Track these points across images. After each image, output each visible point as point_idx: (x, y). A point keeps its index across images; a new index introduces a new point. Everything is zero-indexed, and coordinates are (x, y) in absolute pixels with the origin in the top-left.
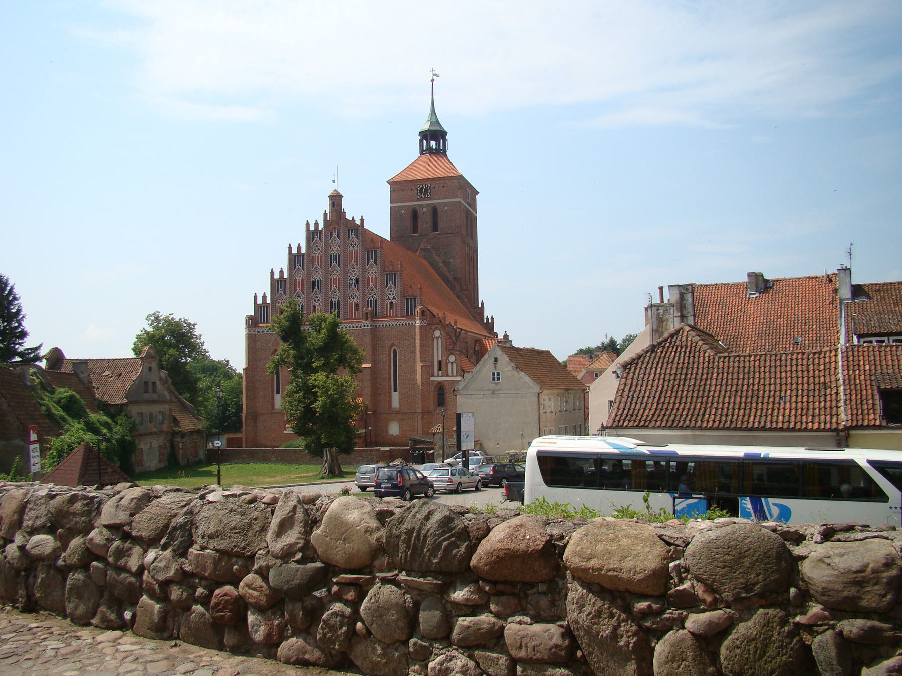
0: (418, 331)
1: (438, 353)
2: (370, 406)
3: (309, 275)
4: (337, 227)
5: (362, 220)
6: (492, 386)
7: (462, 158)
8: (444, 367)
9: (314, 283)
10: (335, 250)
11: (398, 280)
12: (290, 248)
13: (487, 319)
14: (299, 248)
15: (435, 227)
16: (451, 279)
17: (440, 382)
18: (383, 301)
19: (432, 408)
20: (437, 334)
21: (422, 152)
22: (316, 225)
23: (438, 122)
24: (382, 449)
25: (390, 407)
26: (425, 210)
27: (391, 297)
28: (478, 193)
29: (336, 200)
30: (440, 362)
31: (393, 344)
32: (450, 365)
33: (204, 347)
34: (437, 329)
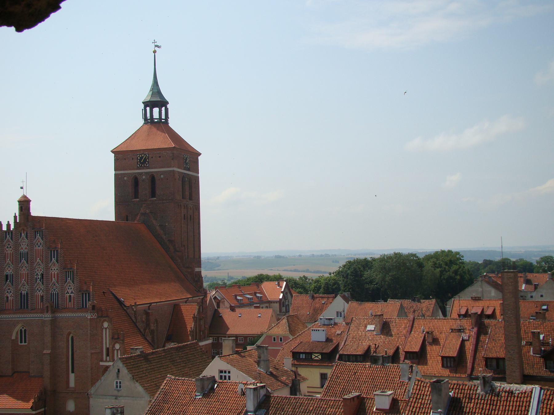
1: (106, 342)
4: (25, 228)
7: (183, 122)
8: (110, 354)
9: (7, 276)
10: (24, 248)
15: (153, 194)
23: (159, 93)
26: (144, 177)
27: (70, 291)
28: (200, 154)
29: (24, 204)
30: (108, 349)
32: (116, 352)
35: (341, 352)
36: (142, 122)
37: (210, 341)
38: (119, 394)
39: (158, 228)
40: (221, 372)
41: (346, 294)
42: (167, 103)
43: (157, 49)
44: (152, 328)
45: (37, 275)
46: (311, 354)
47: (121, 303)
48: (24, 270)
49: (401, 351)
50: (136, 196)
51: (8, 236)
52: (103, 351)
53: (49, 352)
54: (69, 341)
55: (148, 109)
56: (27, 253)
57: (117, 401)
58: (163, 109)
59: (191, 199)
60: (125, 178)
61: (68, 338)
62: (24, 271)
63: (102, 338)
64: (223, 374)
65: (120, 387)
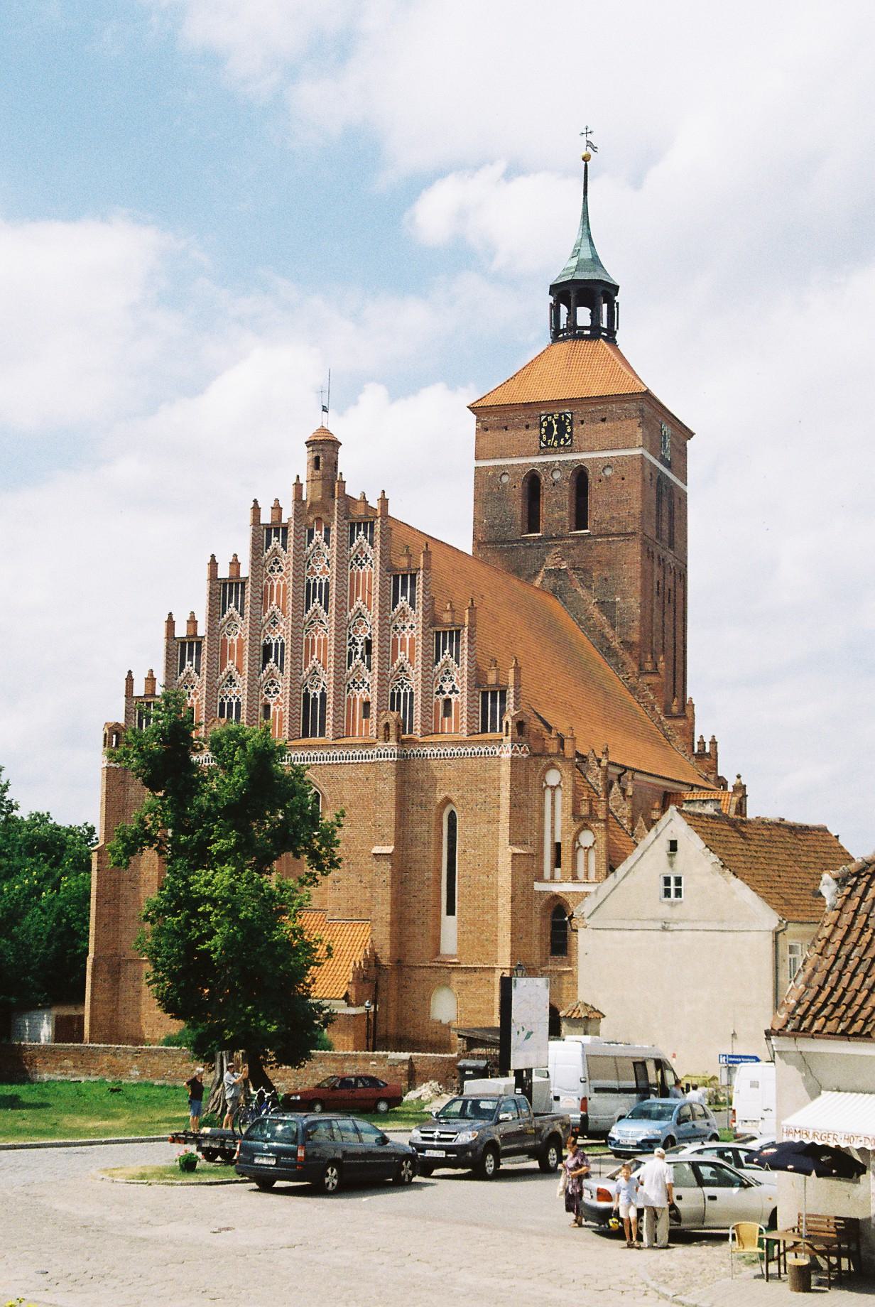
0: (505, 770)
4: (324, 516)
5: (384, 501)
6: (663, 909)
7: (650, 348)
9: (267, 650)
11: (465, 645)
12: (213, 564)
13: (702, 743)
14: (235, 564)
15: (581, 519)
16: (615, 644)
17: (556, 897)
18: (426, 695)
19: (536, 959)
20: (553, 778)
21: (557, 334)
23: (595, 260)
24: (393, 1055)
25: (438, 953)
26: (557, 476)
27: (447, 687)
28: (692, 434)
29: (324, 450)
30: (558, 847)
31: (448, 801)
32: (581, 854)
33: (8, 796)
34: (552, 766)
38: (676, 913)
42: (616, 288)
45: (354, 643)
48: (316, 630)
50: (533, 527)
51: (274, 539)
52: (542, 852)
54: (441, 824)
56: (327, 584)
57: (668, 934)
59: (671, 545)
60: (505, 479)
61: (441, 814)
63: (542, 815)
65: (678, 893)
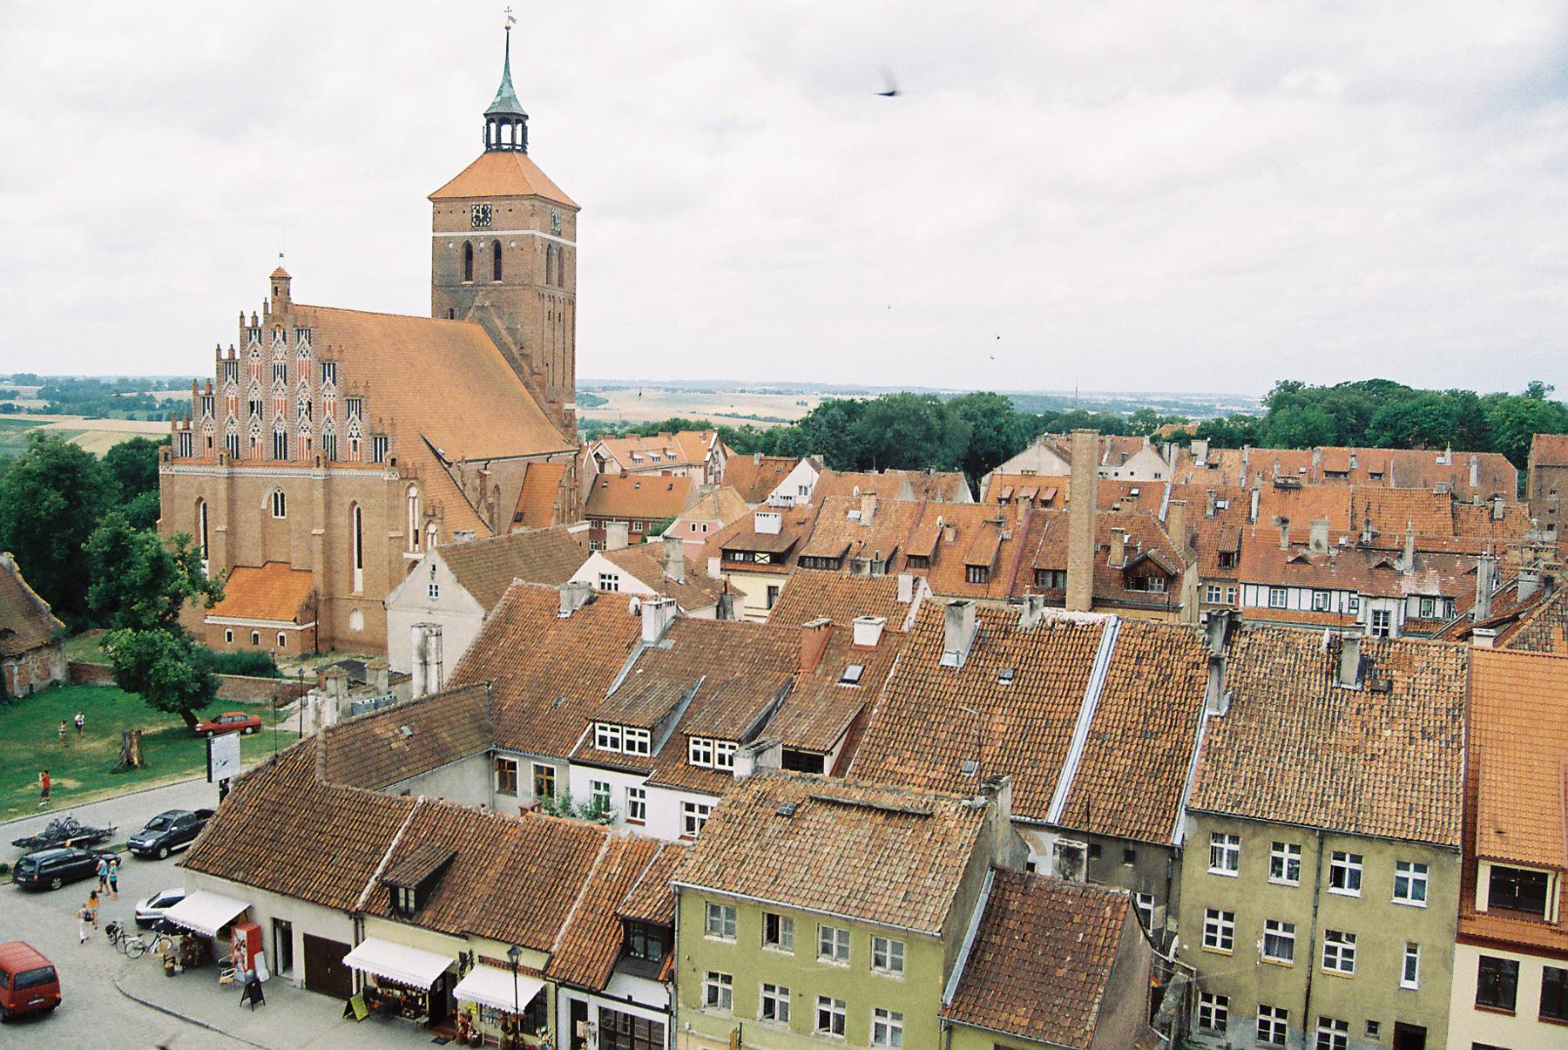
1: (415, 519)
2: (321, 590)
3: (246, 393)
6: (429, 603)
7: (553, 154)
10: (279, 358)
15: (498, 276)
16: (517, 355)
22: (255, 318)
23: (513, 98)
29: (280, 281)
31: (354, 503)
35: (803, 553)
36: (484, 149)
37: (587, 527)
38: (435, 605)
39: (504, 332)
40: (603, 577)
41: (818, 458)
43: (511, 23)
44: (490, 500)
46: (754, 553)
47: (438, 456)
49: (900, 554)
53: (321, 531)
55: (493, 126)
58: (519, 126)
59: (560, 284)
62: (280, 397)
64: (607, 581)
